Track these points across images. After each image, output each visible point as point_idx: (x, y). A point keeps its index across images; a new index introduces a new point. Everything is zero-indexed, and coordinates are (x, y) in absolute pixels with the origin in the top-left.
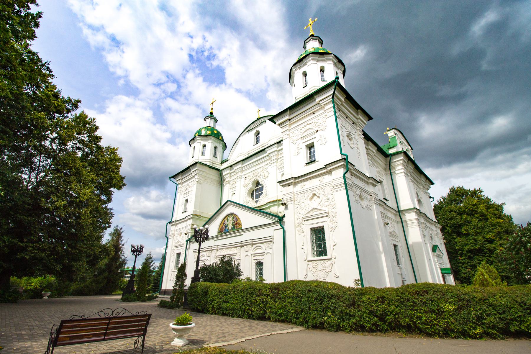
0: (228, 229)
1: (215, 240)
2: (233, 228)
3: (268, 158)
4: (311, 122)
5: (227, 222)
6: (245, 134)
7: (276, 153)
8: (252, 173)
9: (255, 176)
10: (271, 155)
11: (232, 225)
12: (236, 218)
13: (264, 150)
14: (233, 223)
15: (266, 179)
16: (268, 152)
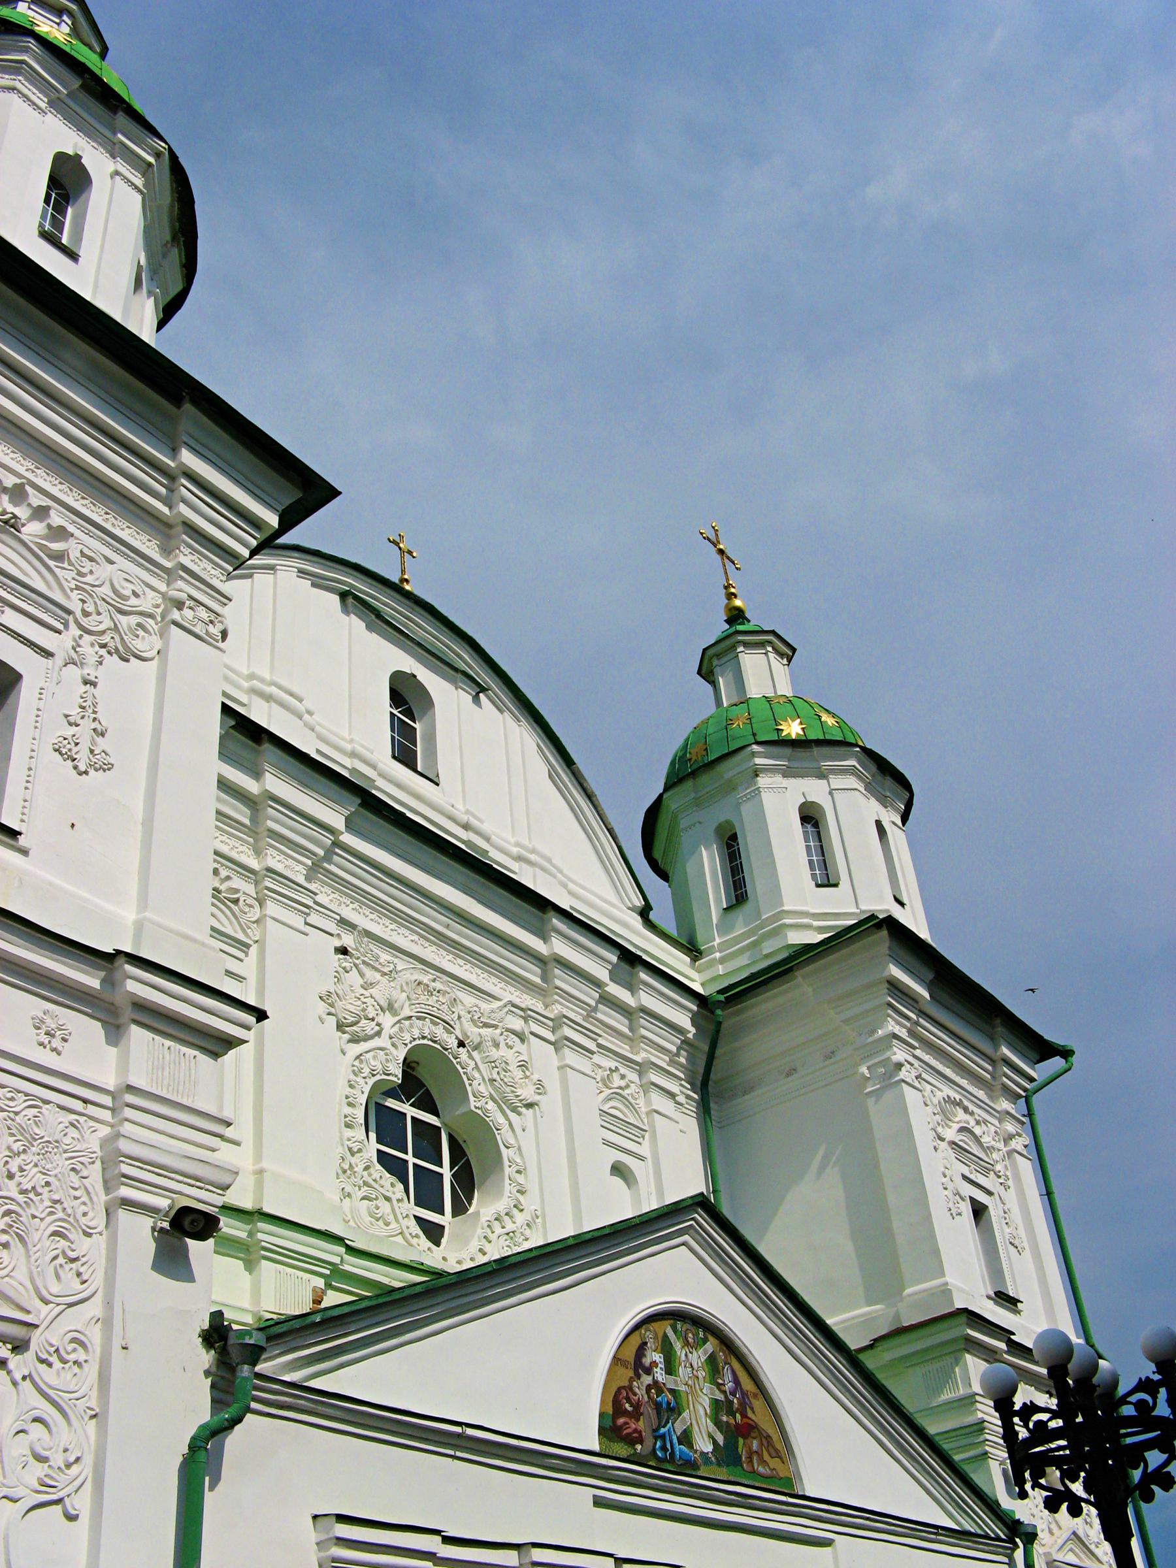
0: (686, 1438)
1: (599, 1502)
2: (727, 1455)
3: (533, 974)
4: (971, 1107)
5: (670, 1370)
6: (319, 583)
7: (590, 996)
8: (409, 973)
9: (436, 1019)
10: (562, 980)
11: (718, 1423)
12: (736, 1380)
13: (542, 904)
14: (716, 1403)
15: (514, 1110)
16: (560, 947)
